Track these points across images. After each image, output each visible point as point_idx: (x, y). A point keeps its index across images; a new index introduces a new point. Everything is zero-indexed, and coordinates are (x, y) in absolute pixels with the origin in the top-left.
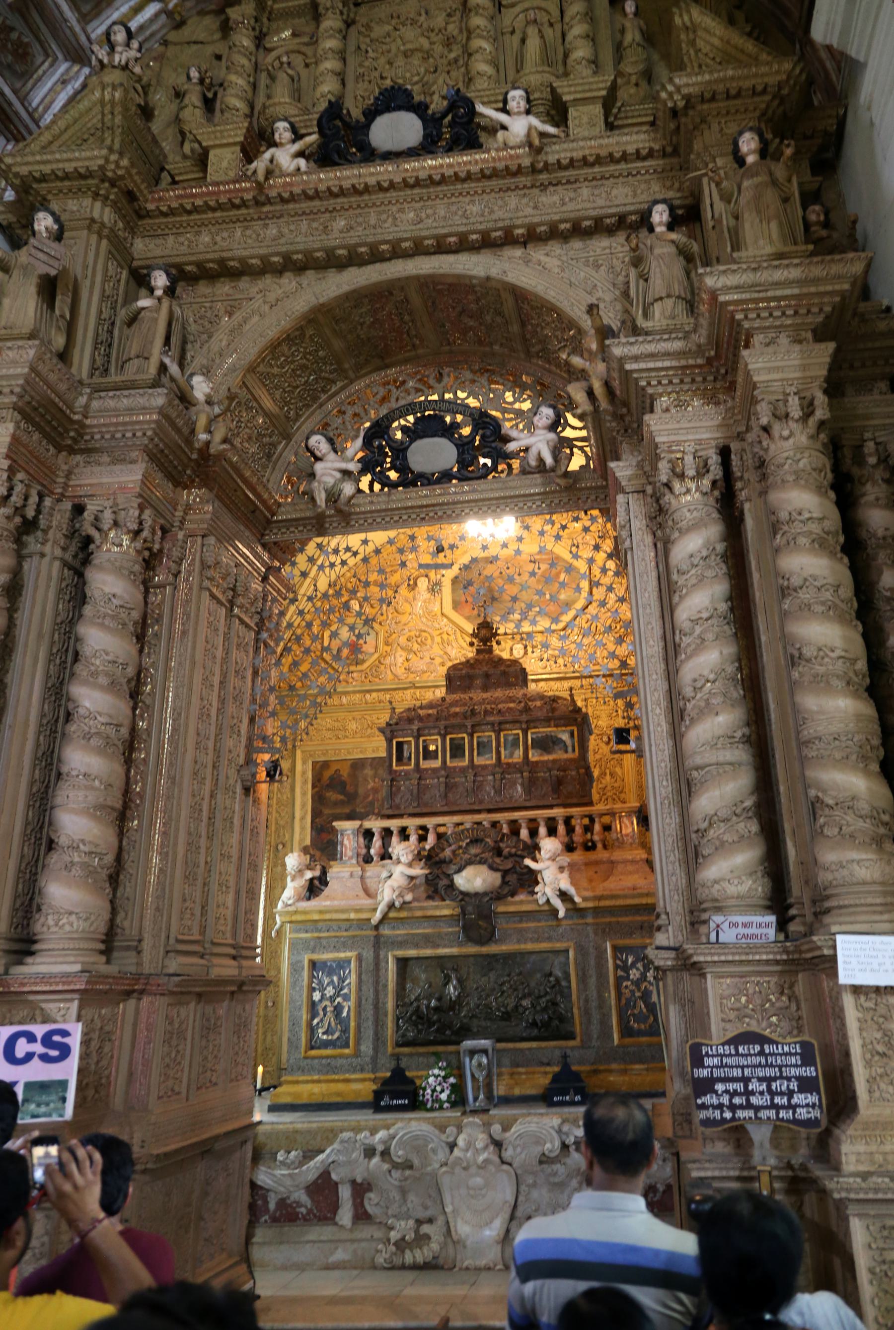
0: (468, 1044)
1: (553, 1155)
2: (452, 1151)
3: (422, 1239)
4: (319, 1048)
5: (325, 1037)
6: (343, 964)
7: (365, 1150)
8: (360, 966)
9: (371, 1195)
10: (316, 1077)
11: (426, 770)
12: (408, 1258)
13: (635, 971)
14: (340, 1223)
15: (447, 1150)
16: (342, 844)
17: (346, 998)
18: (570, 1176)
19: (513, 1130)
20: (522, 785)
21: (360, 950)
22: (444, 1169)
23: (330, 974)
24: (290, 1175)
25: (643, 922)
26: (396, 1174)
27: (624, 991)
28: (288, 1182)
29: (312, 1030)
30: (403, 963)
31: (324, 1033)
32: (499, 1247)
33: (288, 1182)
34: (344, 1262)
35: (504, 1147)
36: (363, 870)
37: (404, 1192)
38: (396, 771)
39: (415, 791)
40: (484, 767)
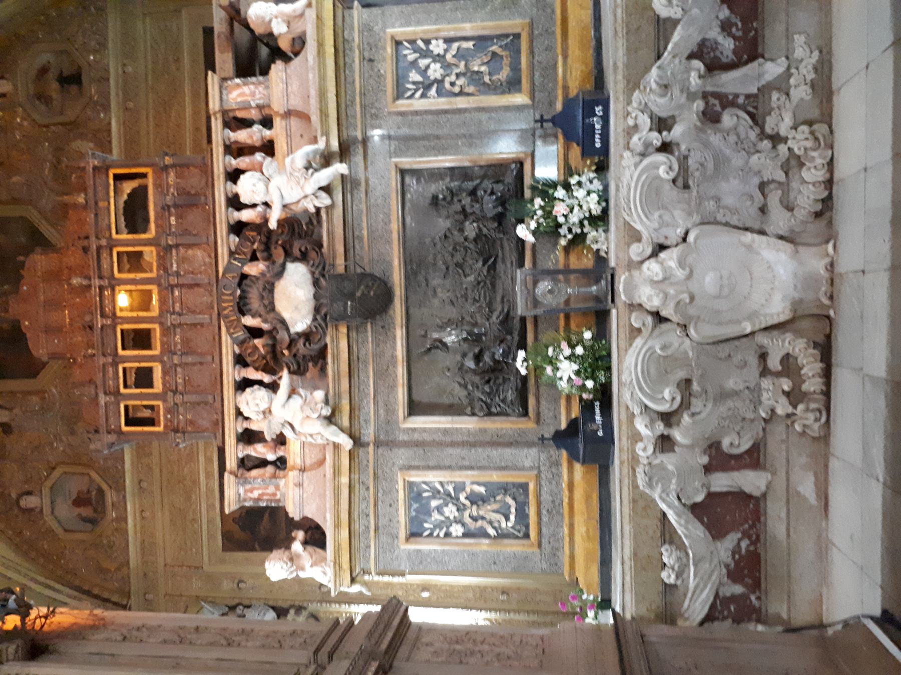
0: (521, 308)
1: (676, 167)
2: (666, 320)
3: (789, 365)
4: (527, 527)
5: (512, 517)
6: (414, 494)
7: (662, 451)
8: (417, 468)
9: (725, 443)
10: (566, 530)
11: (164, 385)
12: (812, 385)
13: (430, 72)
14: (763, 488)
15: (665, 326)
16: (258, 499)
17: (459, 488)
18: (706, 145)
19: (638, 226)
20: (189, 246)
21: (395, 469)
22: (692, 332)
23: (429, 513)
24: (695, 565)
25: (363, 58)
26: (697, 404)
27: (457, 89)
28: (706, 566)
29: (502, 535)
30: (414, 408)
31: (507, 519)
32: (801, 249)
33: (706, 566)
34: (816, 484)
35: (662, 240)
36: (293, 468)
37: (723, 395)
38: (166, 426)
39: (193, 398)
40: (162, 301)
